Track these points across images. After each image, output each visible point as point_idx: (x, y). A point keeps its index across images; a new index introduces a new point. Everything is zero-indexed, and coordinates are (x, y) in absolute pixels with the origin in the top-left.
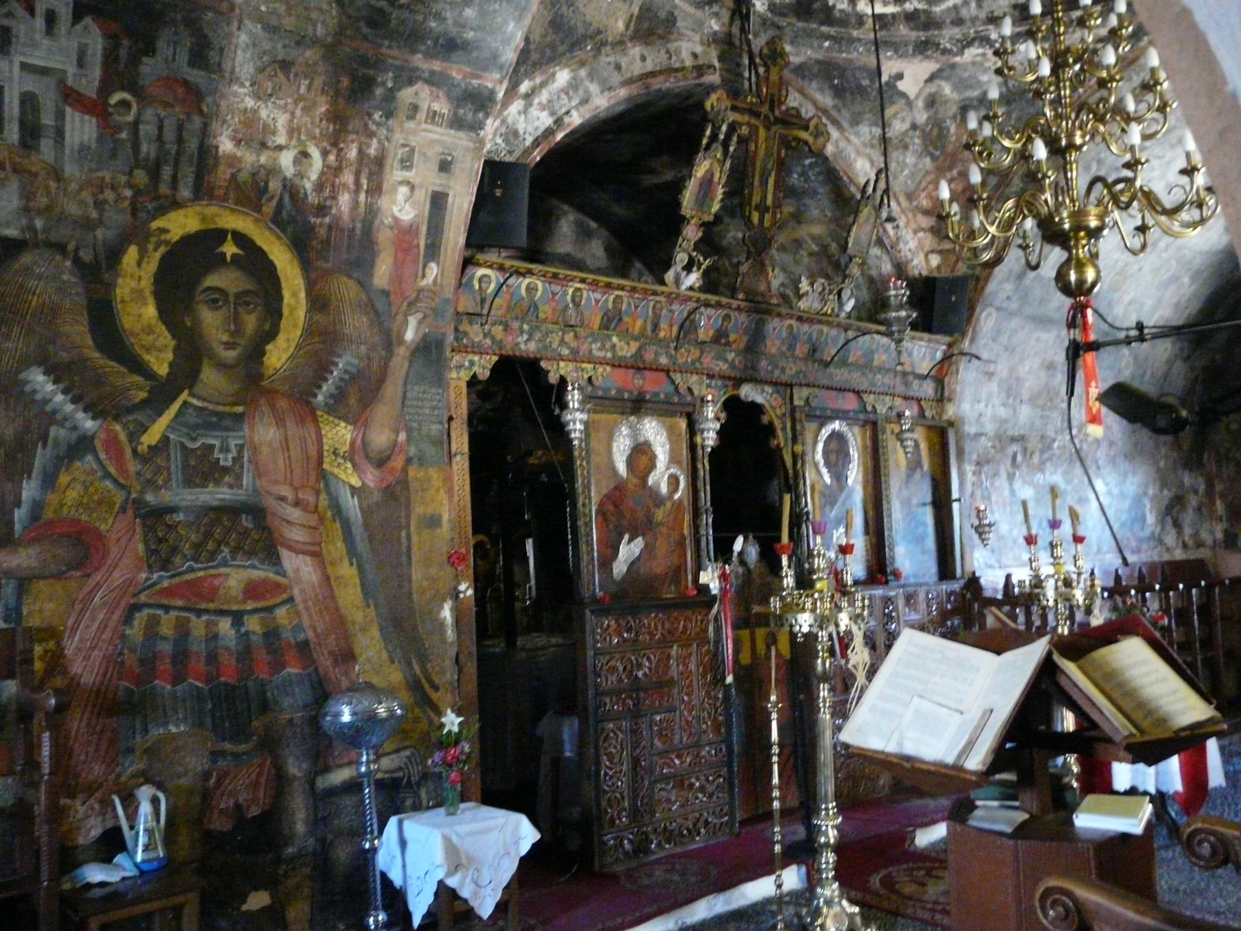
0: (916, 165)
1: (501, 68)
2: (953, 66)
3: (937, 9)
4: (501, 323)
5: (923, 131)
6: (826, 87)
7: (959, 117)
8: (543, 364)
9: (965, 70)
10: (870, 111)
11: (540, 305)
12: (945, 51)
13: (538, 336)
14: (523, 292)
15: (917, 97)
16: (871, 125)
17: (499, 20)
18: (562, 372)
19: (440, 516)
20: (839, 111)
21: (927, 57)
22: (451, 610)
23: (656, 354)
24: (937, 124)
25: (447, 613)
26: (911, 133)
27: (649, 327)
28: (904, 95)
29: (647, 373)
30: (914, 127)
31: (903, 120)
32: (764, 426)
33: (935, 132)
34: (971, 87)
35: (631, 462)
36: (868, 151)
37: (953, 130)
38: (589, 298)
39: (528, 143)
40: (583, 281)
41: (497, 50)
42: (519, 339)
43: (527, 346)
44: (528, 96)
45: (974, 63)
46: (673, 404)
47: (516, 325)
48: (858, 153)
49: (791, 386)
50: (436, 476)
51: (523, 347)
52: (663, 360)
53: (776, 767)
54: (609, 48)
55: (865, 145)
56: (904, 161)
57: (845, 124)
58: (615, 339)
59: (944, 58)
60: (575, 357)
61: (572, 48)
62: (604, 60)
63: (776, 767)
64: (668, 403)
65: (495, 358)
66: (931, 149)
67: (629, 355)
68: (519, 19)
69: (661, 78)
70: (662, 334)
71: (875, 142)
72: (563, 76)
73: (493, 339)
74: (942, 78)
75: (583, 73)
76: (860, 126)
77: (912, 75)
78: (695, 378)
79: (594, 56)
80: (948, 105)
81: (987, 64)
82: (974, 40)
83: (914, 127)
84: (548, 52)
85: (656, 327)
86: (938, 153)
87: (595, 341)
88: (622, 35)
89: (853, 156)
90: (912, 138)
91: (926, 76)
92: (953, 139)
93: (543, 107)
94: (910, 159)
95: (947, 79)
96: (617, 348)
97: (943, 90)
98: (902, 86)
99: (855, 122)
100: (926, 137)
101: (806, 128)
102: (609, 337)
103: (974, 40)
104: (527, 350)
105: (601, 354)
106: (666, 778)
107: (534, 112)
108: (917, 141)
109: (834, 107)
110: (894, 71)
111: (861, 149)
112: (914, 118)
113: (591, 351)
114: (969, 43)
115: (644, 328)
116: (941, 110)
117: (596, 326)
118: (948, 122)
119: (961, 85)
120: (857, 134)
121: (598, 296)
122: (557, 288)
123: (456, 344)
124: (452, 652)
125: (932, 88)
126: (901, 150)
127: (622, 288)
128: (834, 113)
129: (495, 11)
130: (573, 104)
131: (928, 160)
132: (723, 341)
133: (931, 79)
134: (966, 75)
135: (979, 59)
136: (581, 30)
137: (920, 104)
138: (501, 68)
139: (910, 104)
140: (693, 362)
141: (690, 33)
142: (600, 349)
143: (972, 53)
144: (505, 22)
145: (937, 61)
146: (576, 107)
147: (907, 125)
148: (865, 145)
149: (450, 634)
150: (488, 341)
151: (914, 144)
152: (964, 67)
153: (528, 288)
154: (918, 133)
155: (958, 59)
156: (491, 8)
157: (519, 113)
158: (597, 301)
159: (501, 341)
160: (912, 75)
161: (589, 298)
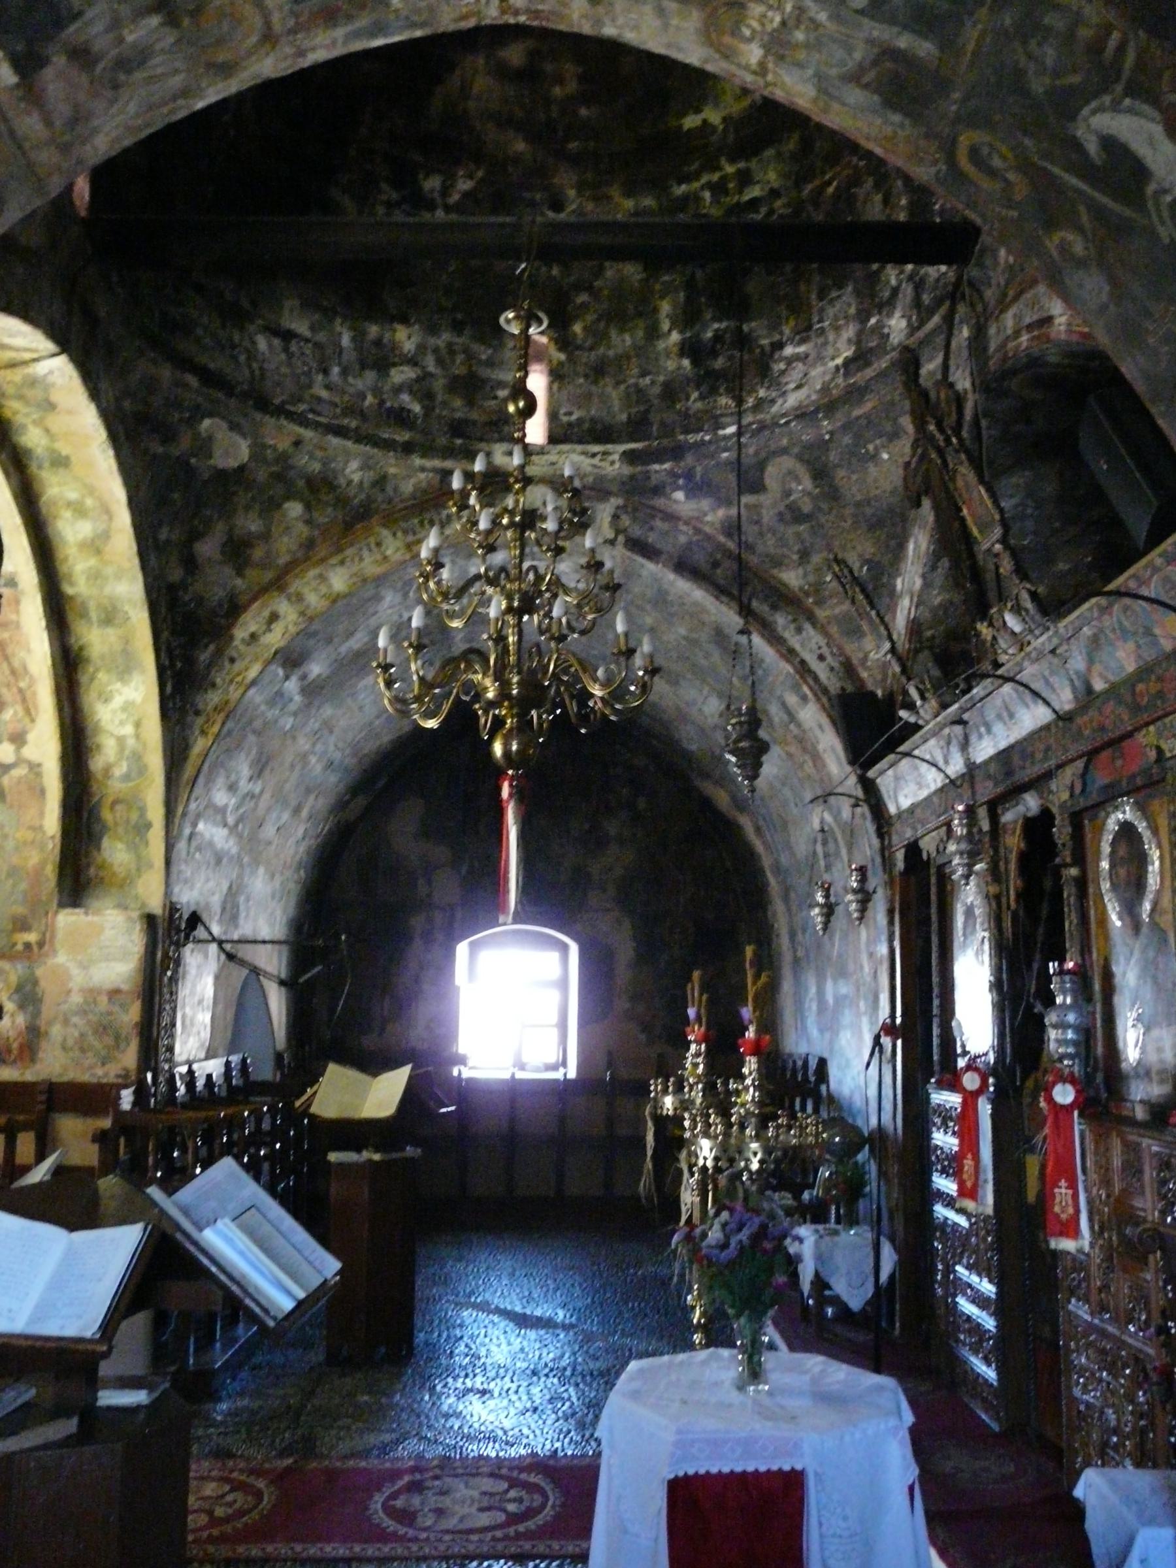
84: (893, 543)
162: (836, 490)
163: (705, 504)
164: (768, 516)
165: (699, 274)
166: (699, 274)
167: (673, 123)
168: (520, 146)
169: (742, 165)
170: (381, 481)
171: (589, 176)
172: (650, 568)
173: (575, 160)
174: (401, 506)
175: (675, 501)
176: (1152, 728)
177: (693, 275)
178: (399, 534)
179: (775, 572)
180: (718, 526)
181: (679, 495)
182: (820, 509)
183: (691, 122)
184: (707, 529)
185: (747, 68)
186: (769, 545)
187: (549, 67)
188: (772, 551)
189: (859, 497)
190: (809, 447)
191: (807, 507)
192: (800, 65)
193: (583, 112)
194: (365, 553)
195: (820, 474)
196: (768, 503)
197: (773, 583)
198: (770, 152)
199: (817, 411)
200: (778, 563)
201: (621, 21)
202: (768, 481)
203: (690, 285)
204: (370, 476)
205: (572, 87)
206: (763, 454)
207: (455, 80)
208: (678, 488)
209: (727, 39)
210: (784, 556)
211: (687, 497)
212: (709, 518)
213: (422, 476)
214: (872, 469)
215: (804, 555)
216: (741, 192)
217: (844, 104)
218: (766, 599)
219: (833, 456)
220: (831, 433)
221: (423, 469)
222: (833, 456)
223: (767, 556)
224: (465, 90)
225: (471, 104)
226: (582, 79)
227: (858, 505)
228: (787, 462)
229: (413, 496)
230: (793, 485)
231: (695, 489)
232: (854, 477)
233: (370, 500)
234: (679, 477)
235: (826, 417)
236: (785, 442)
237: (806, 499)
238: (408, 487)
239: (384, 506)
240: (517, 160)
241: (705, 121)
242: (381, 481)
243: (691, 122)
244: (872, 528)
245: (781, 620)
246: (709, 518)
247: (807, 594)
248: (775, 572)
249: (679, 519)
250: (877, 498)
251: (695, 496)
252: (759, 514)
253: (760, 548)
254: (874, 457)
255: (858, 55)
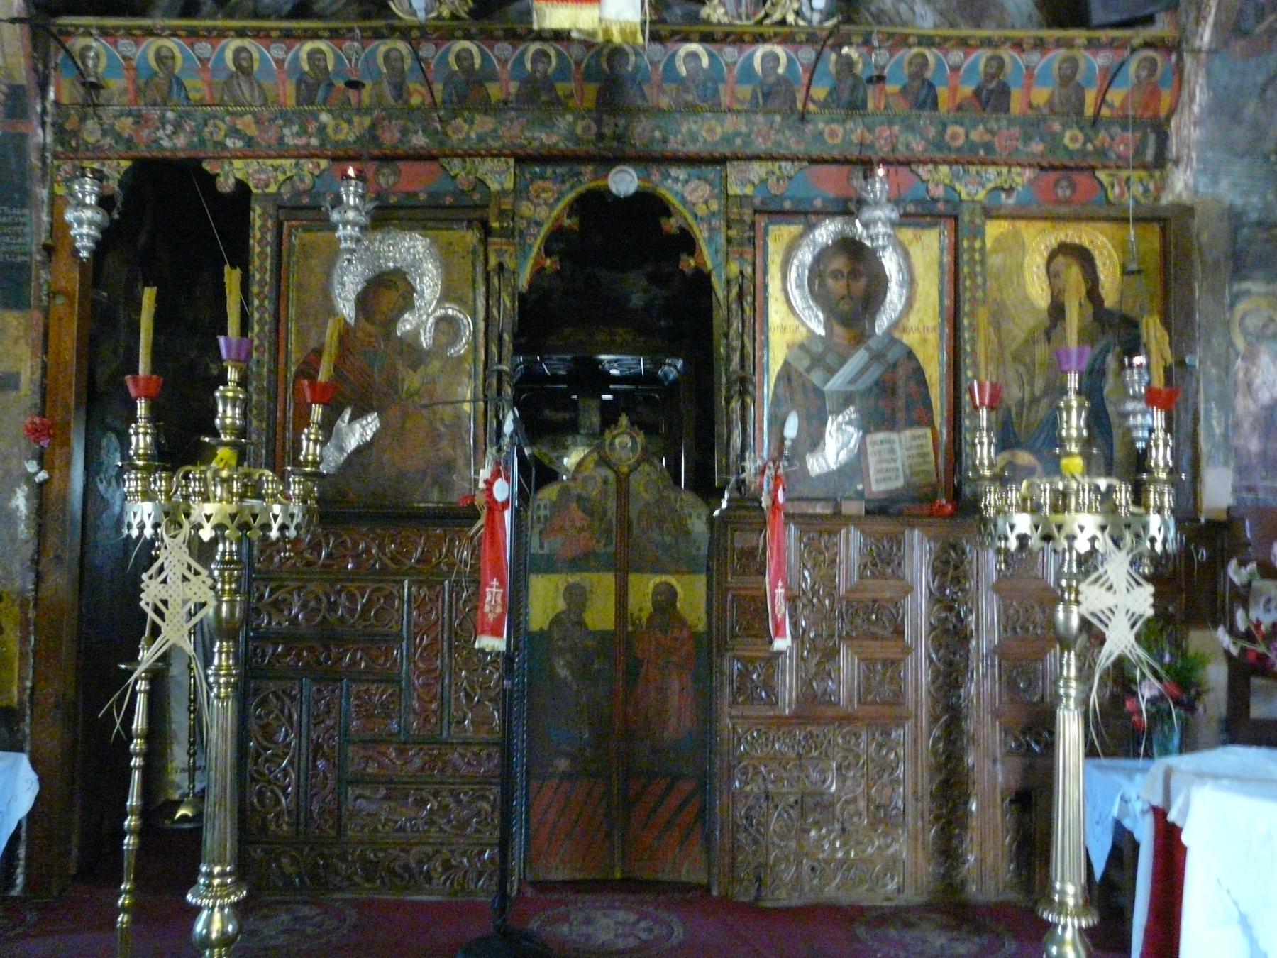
4: (129, 114)
8: (206, 166)
11: (188, 83)
13: (189, 125)
14: (153, 64)
18: (240, 175)
19: (17, 375)
22: (27, 499)
23: (404, 131)
25: (20, 501)
27: (387, 90)
29: (402, 165)
32: (670, 237)
35: (364, 302)
38: (263, 59)
40: (241, 33)
42: (160, 133)
43: (174, 143)
46: (443, 207)
47: (155, 113)
49: (721, 161)
50: (15, 323)
51: (166, 143)
52: (419, 140)
53: (136, 776)
58: (324, 117)
60: (251, 150)
63: (136, 776)
64: (436, 207)
65: (126, 164)
67: (352, 138)
70: (415, 100)
73: (118, 137)
78: (489, 164)
85: (400, 90)
87: (288, 122)
96: (330, 131)
102: (315, 116)
104: (174, 149)
105: (302, 141)
106: (375, 782)
113: (281, 138)
115: (379, 96)
117: (291, 102)
121: (277, 51)
122: (204, 48)
123: (59, 149)
124: (28, 551)
127: (315, 35)
132: (544, 98)
140: (481, 139)
142: (298, 134)
149: (23, 530)
150: (109, 140)
153: (160, 58)
158: (280, 63)
159: (129, 140)
161: (263, 59)
176: (944, 169)
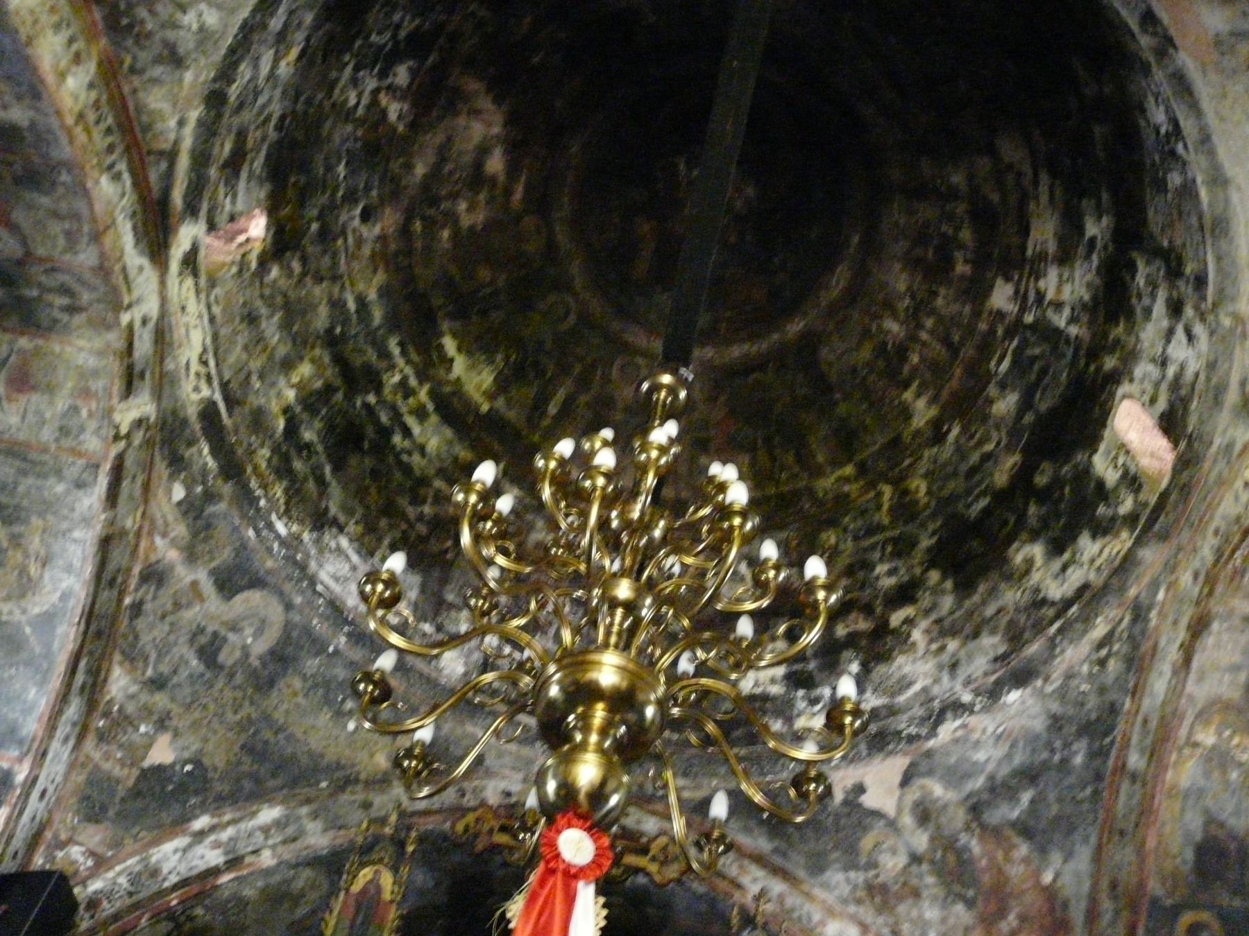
0: (944, 920)
1: (21, 742)
2: (929, 754)
3: (901, 699)
5: (932, 862)
6: (752, 823)
7: (974, 825)
9: (948, 754)
10: (836, 847)
12: (911, 739)
15: (900, 810)
16: (846, 869)
17: (18, 686)
20: (784, 855)
21: (891, 753)
24: (946, 844)
26: (914, 869)
28: (877, 814)
30: (915, 859)
31: (894, 852)
33: (951, 858)
34: (967, 776)
36: (852, 909)
37: (976, 847)
39: (166, 884)
41: (16, 721)
44: (201, 835)
45: (956, 741)
48: (830, 912)
54: (359, 787)
55: (845, 901)
56: (921, 916)
57: (801, 873)
59: (914, 746)
61: (294, 783)
62: (345, 797)
66: (957, 888)
68: (42, 683)
69: (438, 817)
71: (861, 893)
72: (269, 814)
74: (923, 775)
75: (304, 810)
76: (828, 873)
77: (879, 782)
79: (331, 795)
80: (951, 809)
81: (976, 736)
82: (942, 712)
83: (915, 859)
84: (247, 785)
86: (971, 893)
88: (385, 773)
89: (817, 917)
90: (920, 877)
91: (898, 779)
92: (984, 862)
93: (216, 845)
94: (931, 913)
95: (930, 773)
97: (931, 793)
98: (869, 800)
99: (818, 866)
100: (940, 870)
101: (644, 851)
103: (942, 712)
107: (200, 850)
108: (930, 880)
109: (776, 850)
110: (849, 783)
111: (838, 908)
112: (907, 845)
114: (940, 719)
116: (943, 820)
118: (964, 838)
119: (954, 776)
120: (826, 886)
125: (913, 794)
126: (910, 901)
128: (778, 860)
129: (11, 678)
130: (270, 842)
131: (959, 908)
133: (906, 781)
134: (953, 760)
135: (960, 733)
136: (304, 760)
137: (907, 820)
138: (21, 742)
139: (892, 824)
141: (507, 772)
143: (947, 730)
144: (25, 689)
145: (905, 754)
146: (273, 847)
147: (901, 860)
148: (845, 901)
151: (927, 886)
152: (945, 750)
154: (925, 867)
155: (931, 743)
156: (6, 675)
157: (176, 851)
160: (879, 782)
162: (271, 683)
163: (180, 530)
164: (191, 615)
165: (339, 396)
166: (339, 396)
167: (445, 326)
168: (420, 170)
169: (430, 407)
170: (175, 59)
171: (393, 247)
172: (92, 499)
173: (405, 231)
174: (126, 89)
175: (169, 492)
177: (336, 390)
178: (93, 95)
179: (117, 657)
180: (153, 558)
181: (179, 492)
182: (231, 676)
183: (449, 345)
184: (143, 544)
185: (1190, 733)
186: (150, 632)
187: (482, 197)
188: (145, 639)
189: (279, 716)
190: (307, 631)
191: (227, 657)
192: (1207, 775)
193: (446, 234)
194: (65, 34)
195: (281, 658)
196: (212, 609)
197: (105, 665)
198: (448, 433)
199: (350, 623)
200: (133, 658)
201: (1225, 637)
202: (239, 598)
203: (329, 389)
204: (186, 42)
205: (466, 221)
206: (270, 579)
207: (485, 103)
208: (189, 489)
209: (1217, 719)
210: (146, 659)
211: (179, 504)
212: (159, 541)
213: (172, 123)
214: (325, 717)
215: (158, 684)
216: (411, 412)
217: (1183, 810)
218: (89, 672)
219: (312, 664)
220: (336, 652)
221: (181, 123)
222: (312, 664)
223: (136, 637)
224: (476, 113)
225: (462, 121)
226: (472, 228)
227: (267, 718)
228: (275, 613)
229: (139, 109)
230: (249, 631)
231: (192, 509)
232: (300, 699)
233: (142, 38)
234: (204, 483)
235: (349, 635)
236: (298, 600)
237: (238, 654)
238: (156, 100)
239: (128, 61)
240: (409, 167)
241: (452, 360)
242: (175, 59)
243: (449, 345)
244: (248, 749)
245: (73, 710)
246: (159, 541)
247: (106, 714)
248: (117, 657)
249: (146, 502)
250: (290, 738)
251: (185, 514)
252: (189, 605)
253: (141, 624)
254: (340, 715)
255: (1232, 822)
